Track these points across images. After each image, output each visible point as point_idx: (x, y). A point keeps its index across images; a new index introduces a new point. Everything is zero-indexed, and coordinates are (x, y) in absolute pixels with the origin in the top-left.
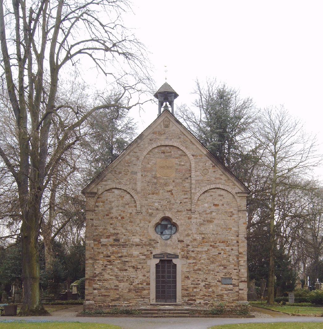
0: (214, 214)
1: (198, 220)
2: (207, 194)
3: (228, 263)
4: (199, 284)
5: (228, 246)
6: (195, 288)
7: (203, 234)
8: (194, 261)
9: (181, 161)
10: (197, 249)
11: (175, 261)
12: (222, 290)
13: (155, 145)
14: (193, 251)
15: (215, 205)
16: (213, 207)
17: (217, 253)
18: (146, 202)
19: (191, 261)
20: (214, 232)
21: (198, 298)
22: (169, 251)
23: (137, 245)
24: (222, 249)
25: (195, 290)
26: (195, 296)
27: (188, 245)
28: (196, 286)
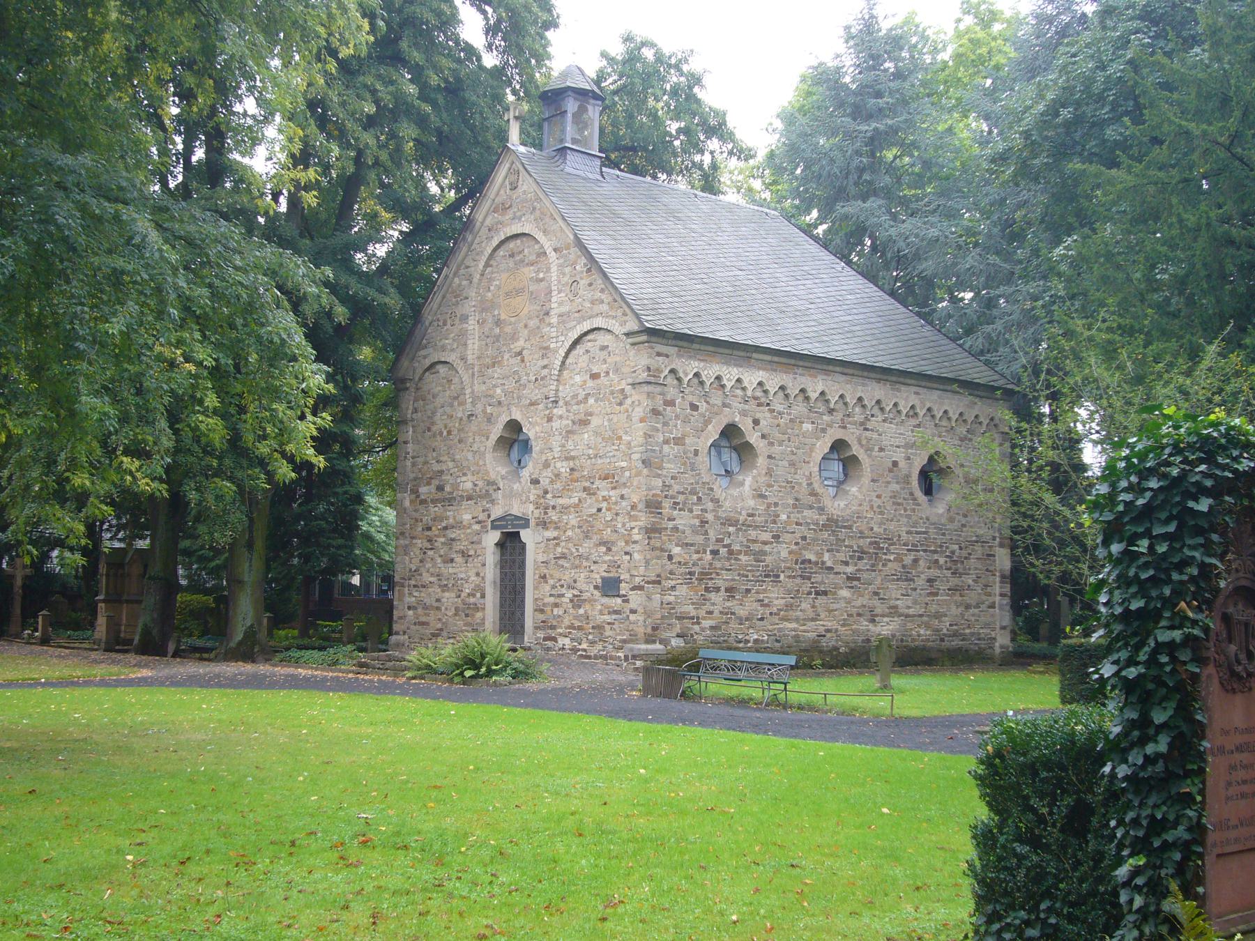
0: (591, 401)
1: (565, 422)
2: (580, 349)
3: (614, 537)
4: (563, 595)
5: (614, 488)
6: (556, 605)
7: (573, 458)
8: (555, 534)
9: (538, 272)
10: (560, 501)
11: (525, 535)
12: (601, 613)
13: (495, 242)
14: (554, 508)
15: (594, 376)
16: (590, 383)
17: (594, 510)
18: (483, 388)
19: (550, 534)
20: (591, 451)
21: (560, 634)
22: (516, 510)
23: (469, 498)
25: (556, 611)
26: (553, 628)
27: (546, 492)
28: (557, 600)
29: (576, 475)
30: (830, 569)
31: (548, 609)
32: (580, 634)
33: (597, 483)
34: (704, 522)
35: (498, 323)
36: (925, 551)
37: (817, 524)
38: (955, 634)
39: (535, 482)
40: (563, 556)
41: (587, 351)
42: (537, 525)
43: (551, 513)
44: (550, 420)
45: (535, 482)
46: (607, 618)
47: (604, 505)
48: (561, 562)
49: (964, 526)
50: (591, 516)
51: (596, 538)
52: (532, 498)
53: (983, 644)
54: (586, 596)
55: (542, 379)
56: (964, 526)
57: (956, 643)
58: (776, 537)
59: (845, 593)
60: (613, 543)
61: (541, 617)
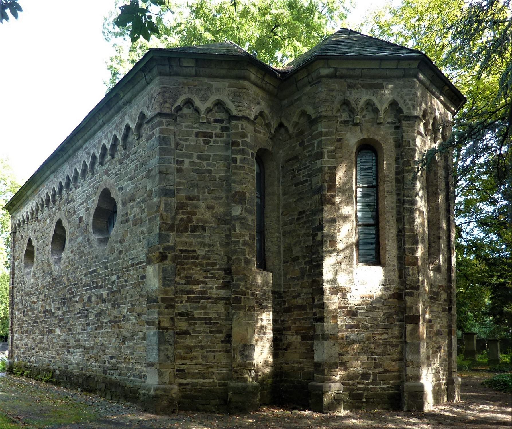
30: (53, 314)
34: (22, 297)
36: (95, 288)
37: (49, 285)
38: (114, 367)
49: (121, 252)
53: (138, 381)
56: (121, 252)
57: (115, 377)
58: (38, 298)
59: (58, 331)
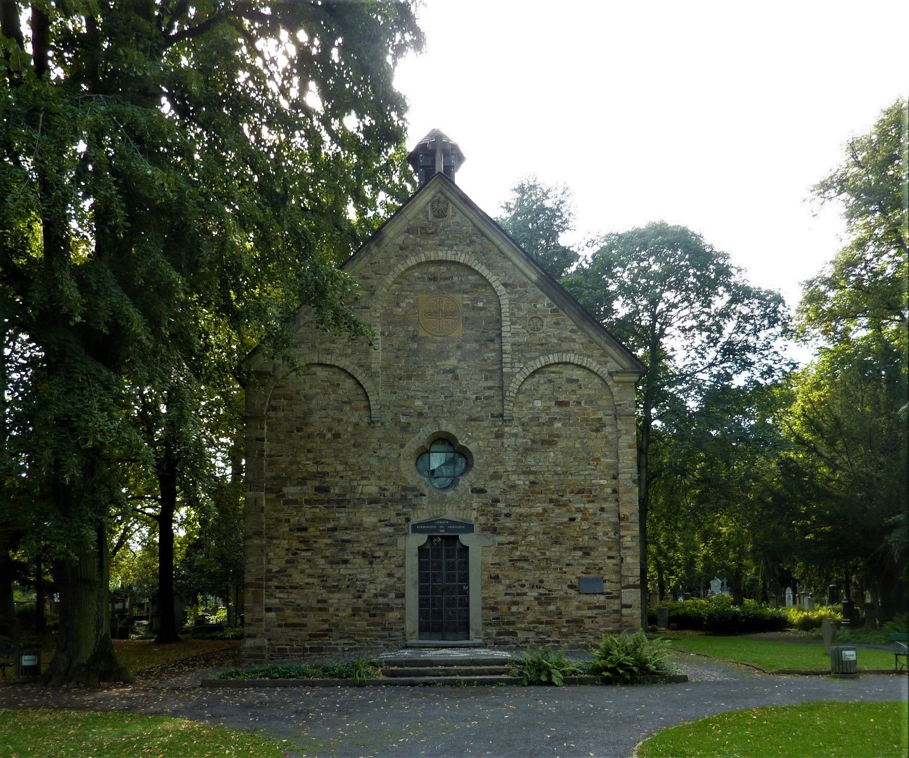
1: (520, 440)
3: (592, 543)
4: (525, 594)
5: (593, 502)
6: (515, 603)
8: (512, 539)
10: (518, 510)
17: (566, 520)
21: (521, 629)
22: (451, 514)
24: (578, 510)
25: (514, 609)
27: (496, 501)
28: (517, 599)
29: (537, 488)
31: (504, 608)
32: (549, 628)
33: (568, 496)
35: (414, 338)
39: (480, 491)
40: (524, 559)
41: (550, 381)
42: (483, 530)
43: (502, 519)
44: (499, 436)
45: (480, 491)
46: (589, 613)
47: (579, 516)
48: (520, 564)
50: (561, 524)
51: (570, 544)
52: (475, 505)
54: (555, 595)
55: (486, 398)
60: (592, 549)
61: (494, 614)
